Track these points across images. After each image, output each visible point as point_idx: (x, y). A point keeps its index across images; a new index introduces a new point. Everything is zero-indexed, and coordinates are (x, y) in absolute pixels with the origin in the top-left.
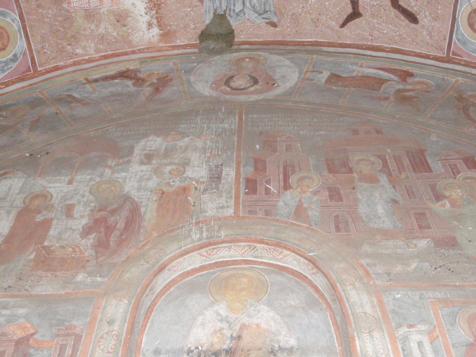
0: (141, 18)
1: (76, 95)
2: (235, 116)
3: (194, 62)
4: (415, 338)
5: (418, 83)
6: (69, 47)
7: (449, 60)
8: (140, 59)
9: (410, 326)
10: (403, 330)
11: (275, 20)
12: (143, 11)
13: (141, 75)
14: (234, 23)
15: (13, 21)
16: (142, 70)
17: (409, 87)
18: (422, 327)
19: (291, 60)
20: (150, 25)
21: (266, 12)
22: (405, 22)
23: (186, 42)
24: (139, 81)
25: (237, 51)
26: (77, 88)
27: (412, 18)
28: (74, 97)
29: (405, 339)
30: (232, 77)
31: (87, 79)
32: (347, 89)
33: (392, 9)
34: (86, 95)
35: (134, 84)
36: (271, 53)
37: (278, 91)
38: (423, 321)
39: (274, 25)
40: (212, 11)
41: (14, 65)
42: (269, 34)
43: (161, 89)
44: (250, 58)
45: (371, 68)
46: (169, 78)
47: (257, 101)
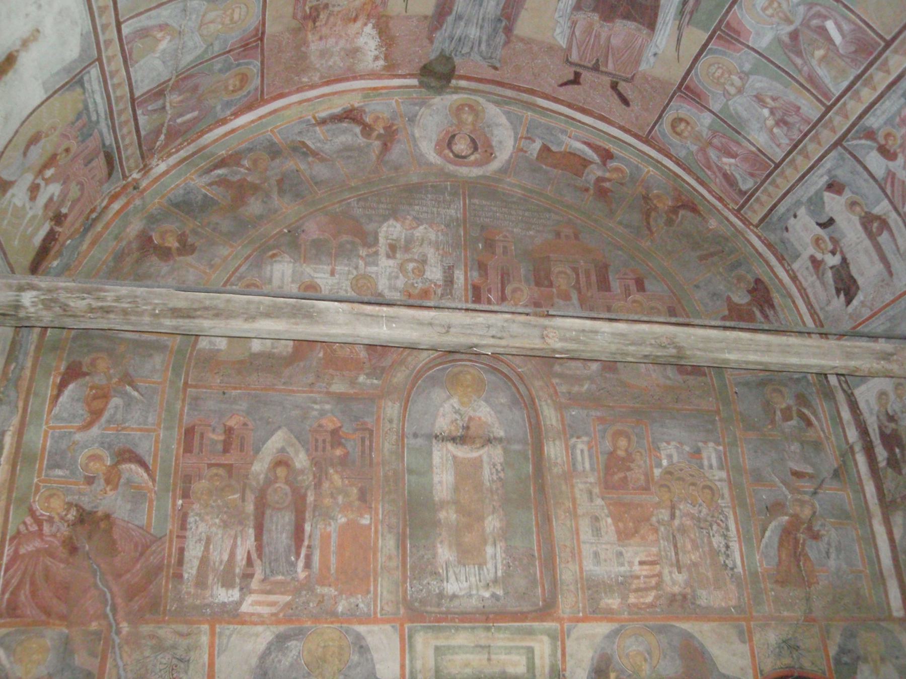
0: (369, 53)
1: (309, 143)
2: (459, 199)
3: (415, 104)
4: (580, 446)
5: (617, 170)
6: (296, 78)
7: (646, 142)
8: (364, 89)
9: (578, 437)
10: (574, 440)
11: (498, 65)
12: (373, 47)
13: (368, 120)
14: (457, 60)
16: (367, 110)
17: (607, 175)
18: (585, 439)
19: (508, 114)
20: (376, 58)
21: (491, 58)
22: (616, 100)
23: (407, 72)
24: (367, 130)
25: (457, 90)
26: (308, 131)
27: (625, 101)
28: (307, 147)
29: (574, 447)
30: (453, 136)
31: (314, 118)
32: (556, 170)
33: (610, 89)
34: (319, 145)
35: (362, 132)
36: (489, 101)
37: (495, 165)
38: (587, 434)
39: (496, 68)
40: (440, 51)
42: (490, 74)
43: (389, 144)
44: (470, 107)
45: (578, 141)
46: (394, 128)
47: (478, 177)
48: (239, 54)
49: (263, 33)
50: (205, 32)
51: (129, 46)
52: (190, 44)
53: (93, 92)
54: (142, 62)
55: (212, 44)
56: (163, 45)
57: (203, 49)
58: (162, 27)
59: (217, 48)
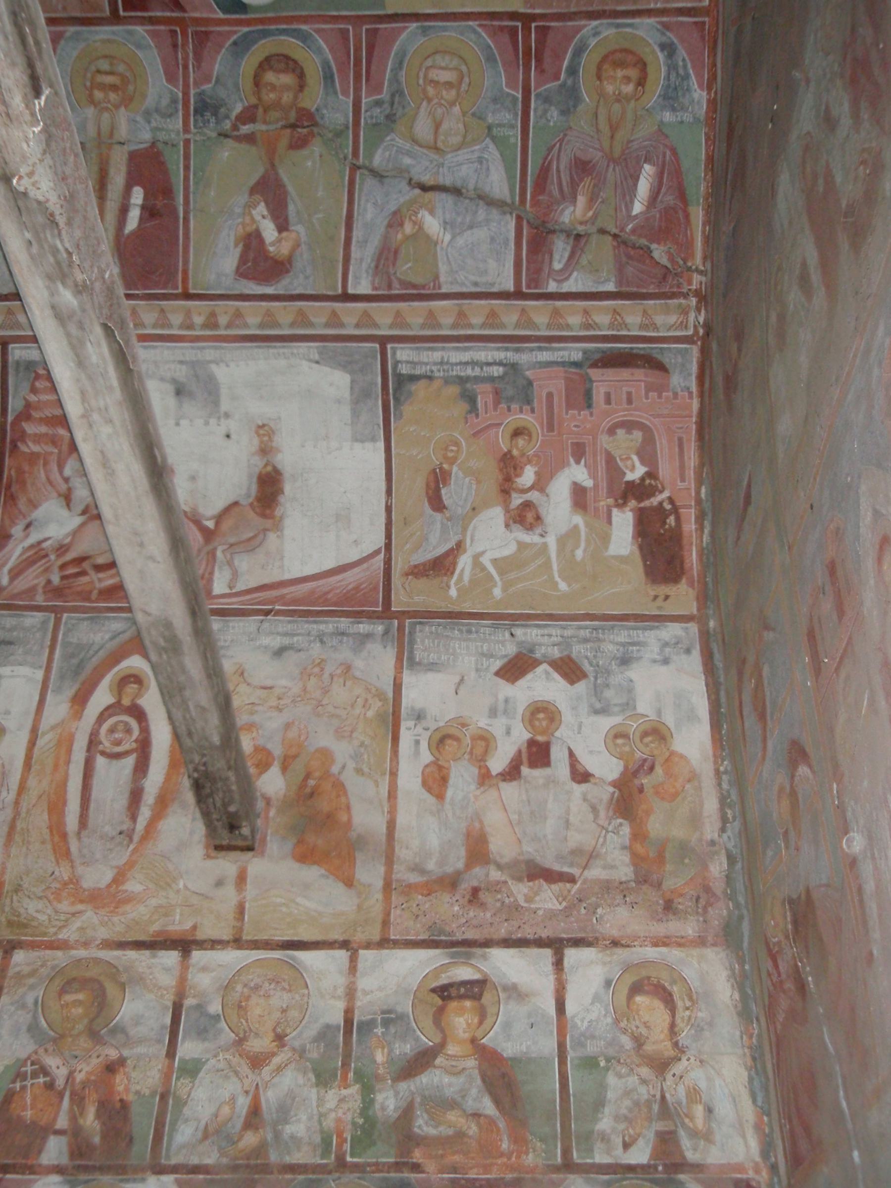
15: (596, 34)
41: (682, 52)
48: (541, 70)
49: (513, 16)
50: (455, 140)
51: (396, 284)
52: (465, 170)
53: (442, 363)
54: (443, 268)
55: (489, 128)
56: (432, 224)
57: (492, 146)
58: (396, 220)
59: (505, 118)
